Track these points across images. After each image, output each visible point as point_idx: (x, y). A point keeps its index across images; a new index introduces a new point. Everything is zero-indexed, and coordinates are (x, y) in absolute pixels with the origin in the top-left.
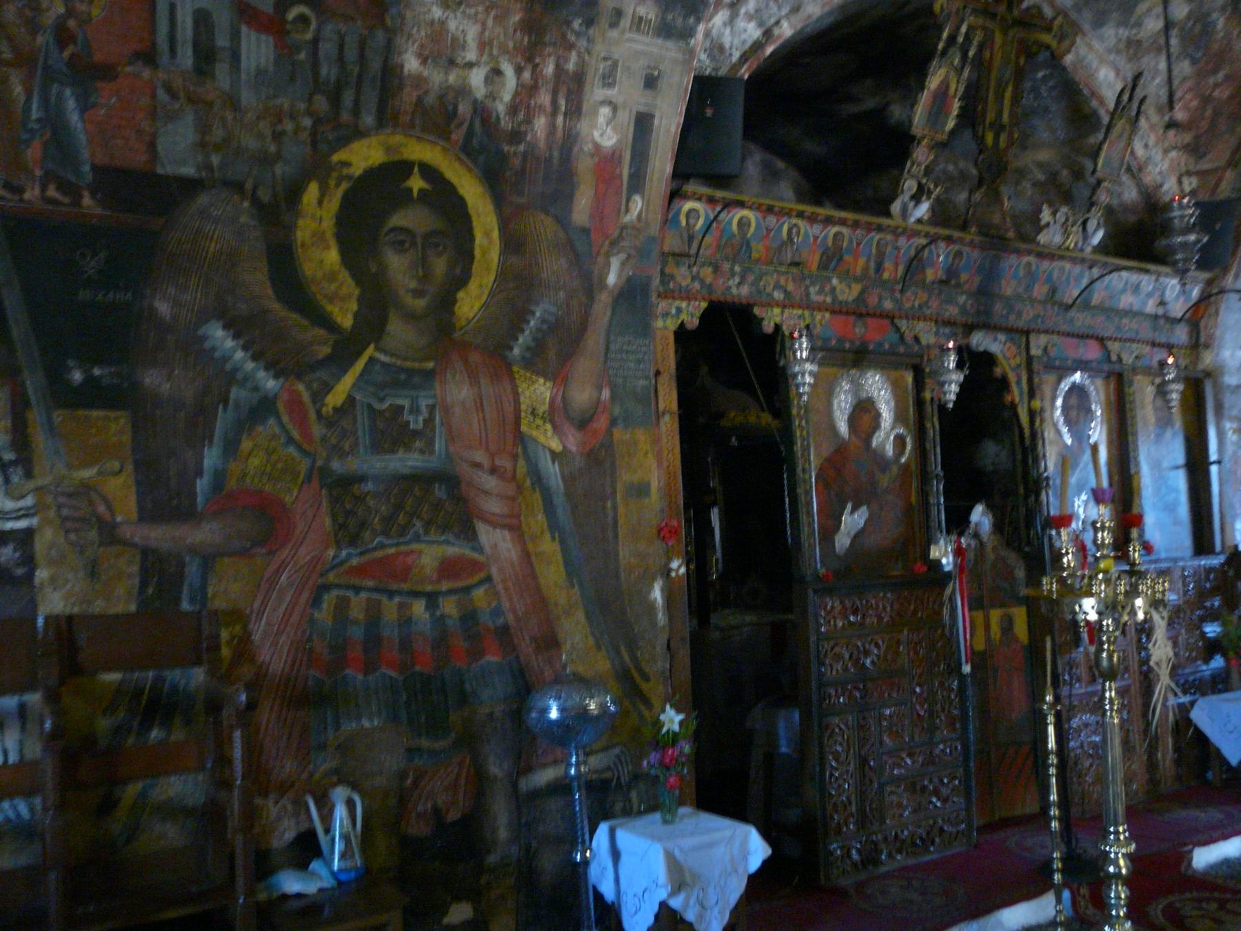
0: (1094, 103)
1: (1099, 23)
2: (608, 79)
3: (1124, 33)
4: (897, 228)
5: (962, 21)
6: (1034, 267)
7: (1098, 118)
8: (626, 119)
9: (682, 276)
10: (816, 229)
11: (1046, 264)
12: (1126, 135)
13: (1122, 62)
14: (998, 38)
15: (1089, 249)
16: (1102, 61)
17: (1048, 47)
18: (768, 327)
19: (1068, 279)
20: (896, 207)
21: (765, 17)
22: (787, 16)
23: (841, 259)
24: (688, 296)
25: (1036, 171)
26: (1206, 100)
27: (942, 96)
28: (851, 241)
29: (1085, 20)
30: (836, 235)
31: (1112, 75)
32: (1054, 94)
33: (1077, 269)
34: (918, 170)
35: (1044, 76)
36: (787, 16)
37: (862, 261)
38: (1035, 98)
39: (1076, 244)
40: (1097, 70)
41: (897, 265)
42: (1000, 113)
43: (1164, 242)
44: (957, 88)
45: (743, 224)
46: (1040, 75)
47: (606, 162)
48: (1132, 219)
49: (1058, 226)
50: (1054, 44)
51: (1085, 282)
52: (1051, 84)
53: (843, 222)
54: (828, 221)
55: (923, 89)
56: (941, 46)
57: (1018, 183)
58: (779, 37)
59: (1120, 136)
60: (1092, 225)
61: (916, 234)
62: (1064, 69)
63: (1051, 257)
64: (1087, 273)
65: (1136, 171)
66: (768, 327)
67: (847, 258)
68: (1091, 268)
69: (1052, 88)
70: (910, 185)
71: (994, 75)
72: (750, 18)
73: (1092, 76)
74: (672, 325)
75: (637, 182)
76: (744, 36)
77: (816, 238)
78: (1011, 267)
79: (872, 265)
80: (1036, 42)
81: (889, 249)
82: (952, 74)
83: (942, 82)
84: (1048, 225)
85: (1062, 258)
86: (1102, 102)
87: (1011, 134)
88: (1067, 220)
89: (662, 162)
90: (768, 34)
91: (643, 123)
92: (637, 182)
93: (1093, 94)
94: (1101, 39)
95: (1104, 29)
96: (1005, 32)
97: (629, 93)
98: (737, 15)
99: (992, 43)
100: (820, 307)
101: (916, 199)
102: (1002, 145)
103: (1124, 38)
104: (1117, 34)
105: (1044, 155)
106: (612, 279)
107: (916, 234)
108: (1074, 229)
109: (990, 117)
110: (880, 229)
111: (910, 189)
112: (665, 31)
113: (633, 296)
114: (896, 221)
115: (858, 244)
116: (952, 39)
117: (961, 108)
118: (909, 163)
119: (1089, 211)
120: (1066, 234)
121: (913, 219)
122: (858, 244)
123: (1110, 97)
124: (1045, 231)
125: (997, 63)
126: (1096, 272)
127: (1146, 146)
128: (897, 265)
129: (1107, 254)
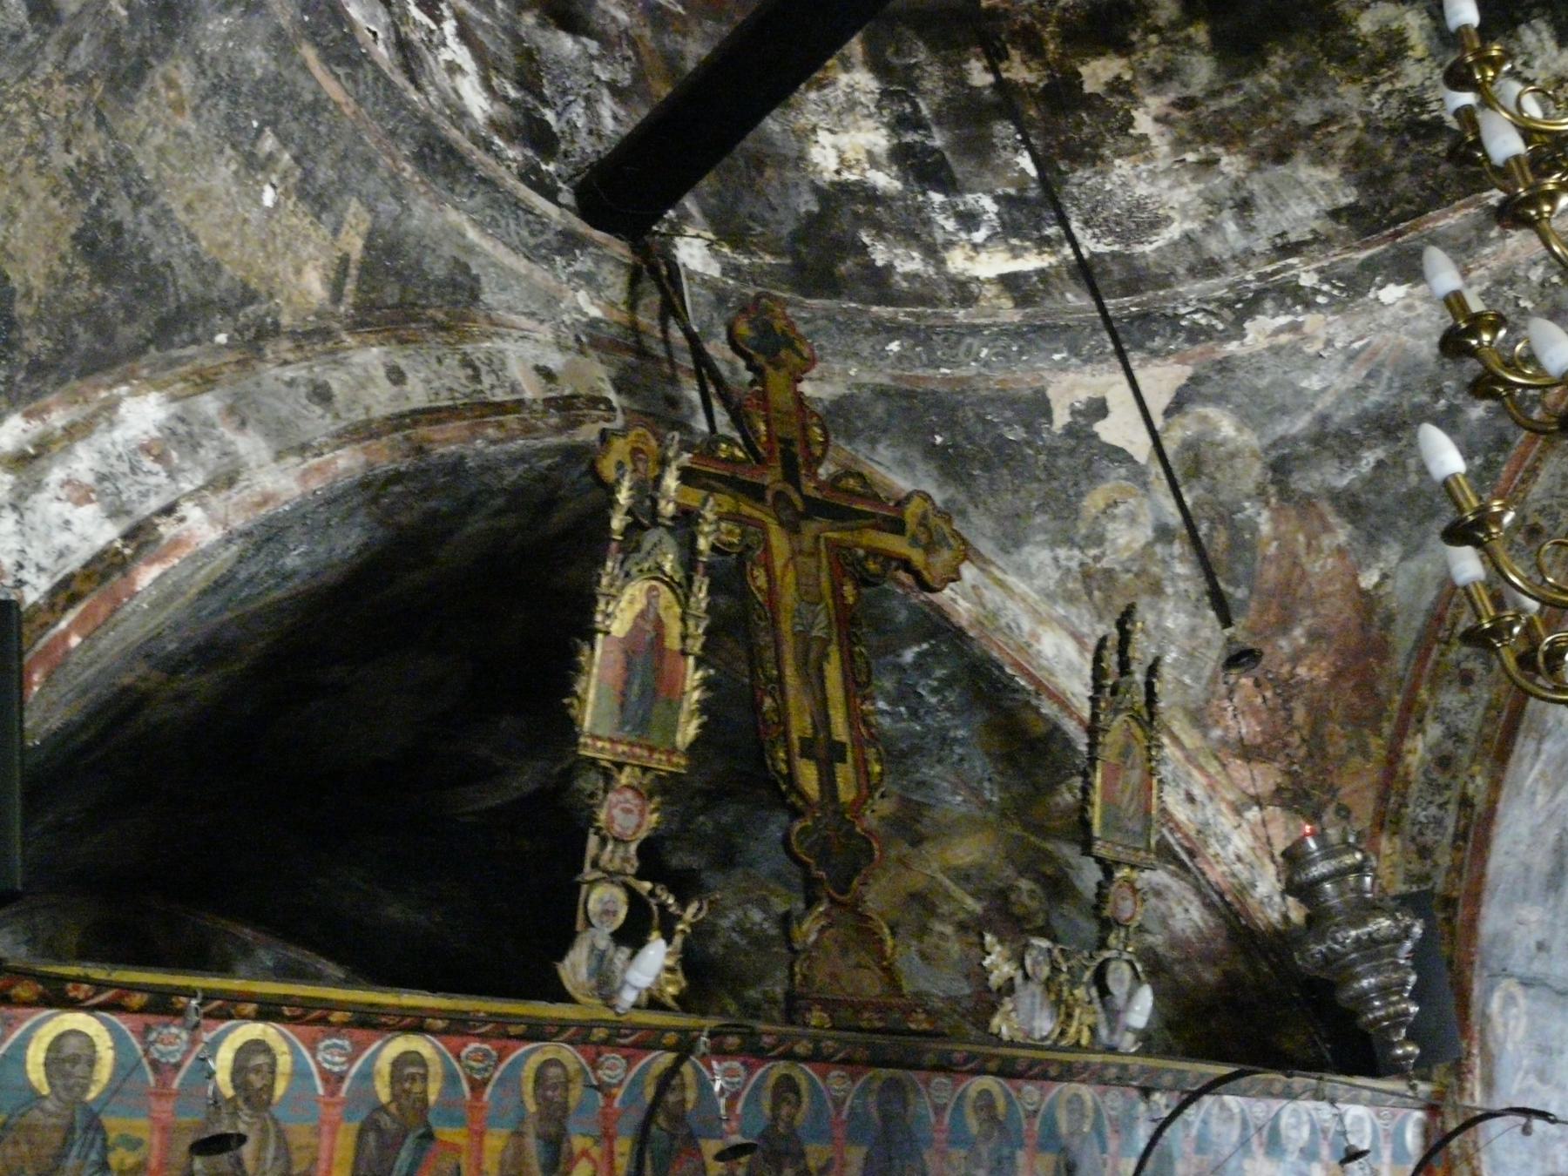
0: (1048, 708)
1: (1012, 540)
3: (1071, 557)
4: (586, 1027)
5: (663, 463)
6: (1001, 1104)
7: (1068, 743)
10: (332, 1053)
11: (1030, 1090)
12: (1138, 752)
14: (779, 541)
15: (1128, 1042)
17: (906, 565)
19: (1097, 1128)
20: (575, 968)
21: (130, 493)
22: (196, 495)
23: (429, 1136)
25: (957, 892)
27: (647, 649)
28: (451, 1078)
29: (979, 528)
30: (399, 1063)
31: (1070, 648)
32: (952, 697)
33: (1115, 1100)
34: (623, 858)
35: (920, 655)
36: (196, 495)
37: (496, 1142)
38: (914, 714)
39: (1093, 1030)
40: (1035, 636)
41: (607, 1137)
42: (822, 720)
43: (1318, 949)
44: (683, 629)
45: (68, 1060)
46: (909, 655)
48: (1210, 976)
49: (1036, 988)
50: (917, 557)
51: (1143, 1133)
52: (940, 672)
53: (416, 1024)
54: (369, 1022)
55: (589, 634)
56: (617, 523)
57: (923, 931)
58: (177, 543)
59: (1125, 752)
60: (1119, 979)
61: (649, 1041)
62: (960, 633)
63: (1039, 1072)
64: (1142, 1107)
65: (1181, 858)
67: (447, 1133)
68: (1146, 1092)
69: (947, 683)
70: (604, 901)
71: (786, 626)
72: (81, 494)
73: (1025, 648)
76: (61, 539)
77: (333, 1080)
78: (939, 1110)
79: (532, 1145)
80: (873, 553)
81: (576, 1093)
82: (666, 595)
83: (642, 615)
84: (1009, 988)
85: (1068, 1073)
86: (1065, 705)
87: (862, 766)
88: (1055, 969)
90: (140, 536)
93: (1041, 687)
94: (1024, 571)
95: (1027, 549)
96: (792, 529)
98: (38, 486)
99: (767, 549)
101: (632, 936)
102: (846, 794)
103: (1074, 565)
104: (1056, 559)
105: (968, 851)
107: (649, 1041)
108: (1080, 992)
109: (800, 725)
110: (536, 1032)
111: (609, 913)
114: (588, 1008)
115: (477, 1087)
116: (644, 517)
117: (706, 683)
118: (593, 842)
119: (1103, 944)
120: (1063, 1009)
121: (629, 997)
122: (477, 1087)
123: (1078, 688)
124: (1008, 1004)
125: (789, 596)
126: (1162, 1102)
127: (1191, 799)
128: (607, 1137)
129: (1168, 1052)
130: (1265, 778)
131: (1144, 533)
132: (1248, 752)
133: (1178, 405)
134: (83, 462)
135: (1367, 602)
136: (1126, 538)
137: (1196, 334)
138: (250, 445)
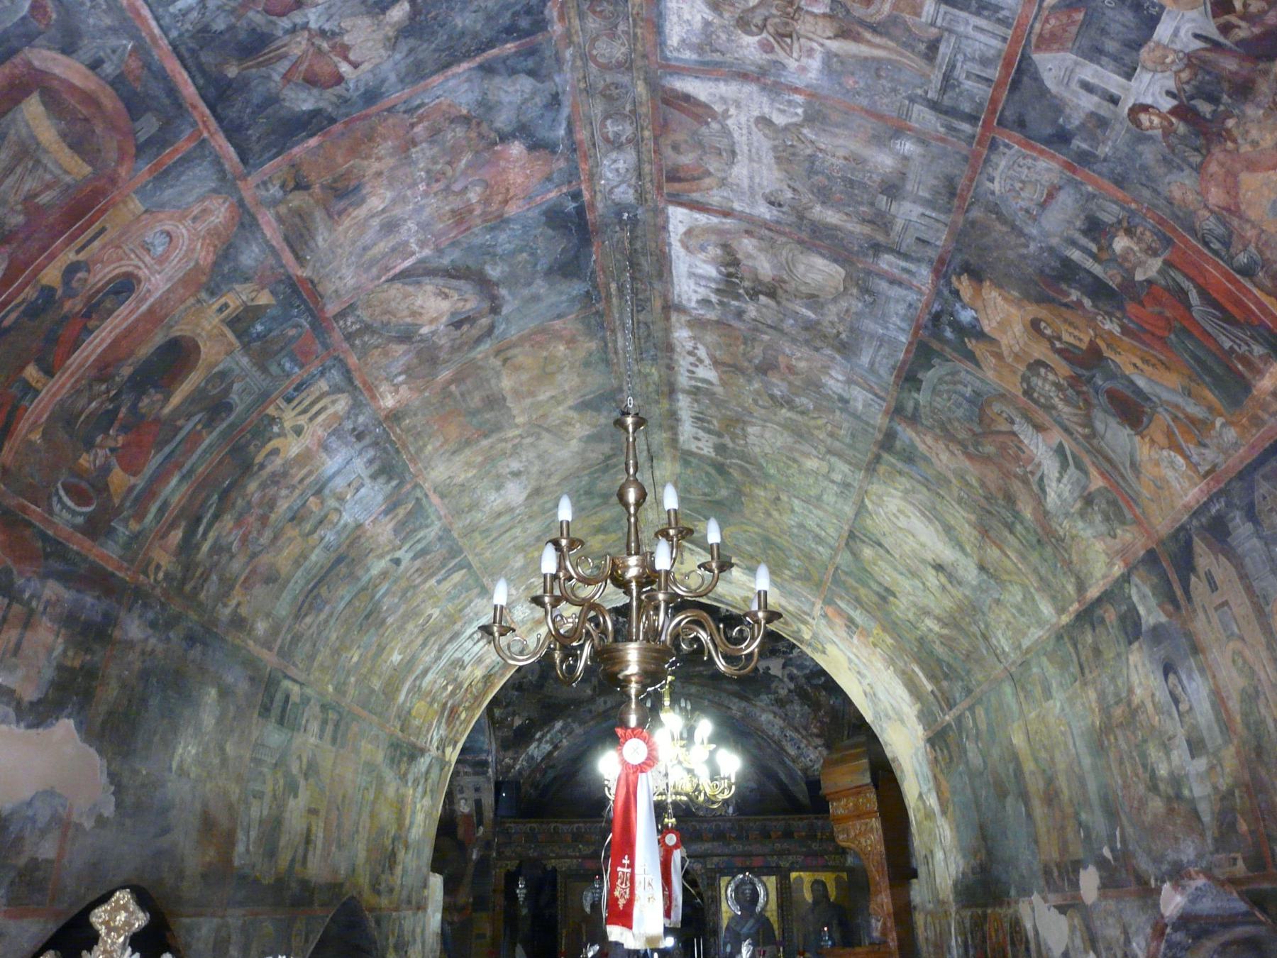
1: (757, 695)
2: (462, 792)
3: (772, 697)
8: (471, 802)
9: (508, 852)
13: (775, 709)
16: (763, 711)
18: (549, 867)
24: (510, 859)
26: (821, 722)
31: (771, 717)
47: (468, 816)
66: (549, 867)
74: (503, 871)
75: (480, 823)
89: (489, 814)
91: (478, 803)
92: (480, 823)
97: (470, 794)
100: (576, 857)
106: (474, 857)
112: (476, 774)
113: (483, 862)
130: (819, 741)
131: (786, 691)
132: (818, 736)
133: (784, 666)
134: (549, 736)
135: (833, 707)
136: (783, 693)
137: (784, 653)
138: (575, 726)
